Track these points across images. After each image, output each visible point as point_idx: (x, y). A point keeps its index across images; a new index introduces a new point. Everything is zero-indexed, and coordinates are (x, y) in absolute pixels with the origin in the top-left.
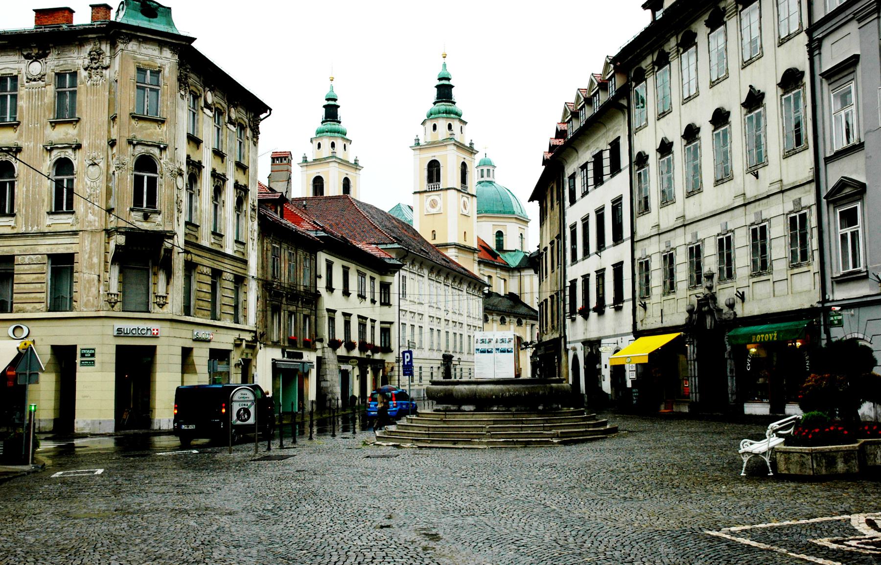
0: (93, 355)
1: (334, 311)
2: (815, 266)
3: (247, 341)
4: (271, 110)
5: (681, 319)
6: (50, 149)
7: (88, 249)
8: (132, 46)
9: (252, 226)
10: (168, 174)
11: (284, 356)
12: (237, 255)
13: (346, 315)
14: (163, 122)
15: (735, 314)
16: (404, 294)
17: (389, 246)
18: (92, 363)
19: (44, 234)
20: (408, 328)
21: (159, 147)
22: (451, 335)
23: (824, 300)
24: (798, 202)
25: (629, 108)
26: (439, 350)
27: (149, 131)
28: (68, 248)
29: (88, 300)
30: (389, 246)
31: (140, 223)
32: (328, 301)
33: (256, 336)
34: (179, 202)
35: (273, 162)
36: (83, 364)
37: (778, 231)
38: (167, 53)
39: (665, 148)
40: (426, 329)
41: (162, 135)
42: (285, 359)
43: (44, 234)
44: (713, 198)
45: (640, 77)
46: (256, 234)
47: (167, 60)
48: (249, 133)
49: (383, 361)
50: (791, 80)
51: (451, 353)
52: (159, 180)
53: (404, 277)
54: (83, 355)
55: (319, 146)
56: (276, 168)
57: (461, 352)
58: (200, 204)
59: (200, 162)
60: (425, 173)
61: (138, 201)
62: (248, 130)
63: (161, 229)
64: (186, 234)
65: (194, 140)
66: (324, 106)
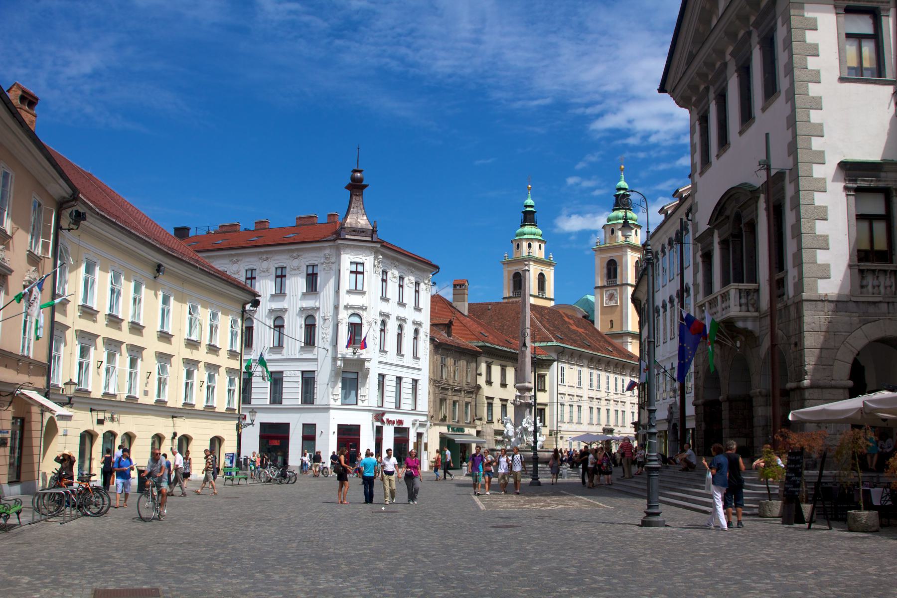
1: (492, 398)
6: (303, 310)
9: (425, 346)
13: (504, 401)
16: (563, 381)
20: (567, 408)
22: (612, 413)
26: (599, 424)
30: (549, 344)
32: (486, 391)
35: (455, 286)
39: (664, 306)
40: (585, 406)
51: (612, 427)
53: (563, 369)
55: (518, 245)
57: (623, 426)
60: (605, 271)
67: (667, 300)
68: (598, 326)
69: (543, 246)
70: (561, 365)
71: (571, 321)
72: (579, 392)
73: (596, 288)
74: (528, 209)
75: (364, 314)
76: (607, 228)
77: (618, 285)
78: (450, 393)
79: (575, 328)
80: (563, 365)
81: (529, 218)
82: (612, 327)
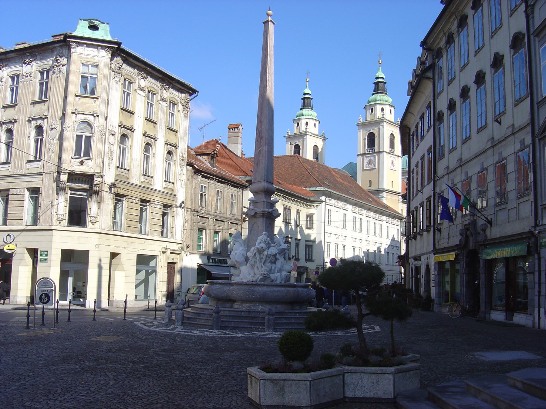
0: (47, 255)
2: (532, 198)
3: (171, 250)
4: (197, 92)
5: (455, 240)
7: (47, 184)
8: (80, 49)
10: (99, 134)
11: (209, 262)
12: (166, 191)
14: (97, 98)
15: (486, 236)
17: (318, 189)
18: (46, 261)
19: (25, 175)
21: (93, 115)
23: (536, 225)
24: (522, 142)
25: (433, 78)
27: (87, 105)
28: (37, 184)
29: (46, 218)
30: (318, 189)
31: (78, 167)
33: (182, 248)
34: (111, 153)
36: (41, 261)
37: (511, 167)
38: (103, 52)
41: (96, 108)
42: (210, 263)
43: (25, 175)
44: (478, 142)
45: (438, 54)
46: (184, 177)
47: (102, 56)
48: (180, 107)
49: (306, 268)
50: (517, 42)
52: (94, 139)
54: (41, 255)
55: (298, 123)
56: (231, 135)
58: (131, 155)
59: (132, 127)
61: (78, 153)
62: (180, 105)
63: (92, 170)
64: (116, 175)
65: (126, 111)
66: (302, 99)
67: (456, 97)
68: (359, 182)
69: (317, 123)
70: (328, 207)
71: (338, 176)
72: (343, 232)
73: (359, 155)
74: (307, 96)
75: (97, 123)
76: (368, 108)
77: (376, 153)
78: (210, 222)
79: (341, 181)
80: (330, 208)
81: (306, 103)
82: (371, 186)
